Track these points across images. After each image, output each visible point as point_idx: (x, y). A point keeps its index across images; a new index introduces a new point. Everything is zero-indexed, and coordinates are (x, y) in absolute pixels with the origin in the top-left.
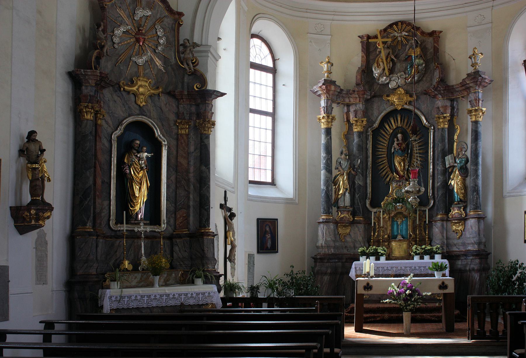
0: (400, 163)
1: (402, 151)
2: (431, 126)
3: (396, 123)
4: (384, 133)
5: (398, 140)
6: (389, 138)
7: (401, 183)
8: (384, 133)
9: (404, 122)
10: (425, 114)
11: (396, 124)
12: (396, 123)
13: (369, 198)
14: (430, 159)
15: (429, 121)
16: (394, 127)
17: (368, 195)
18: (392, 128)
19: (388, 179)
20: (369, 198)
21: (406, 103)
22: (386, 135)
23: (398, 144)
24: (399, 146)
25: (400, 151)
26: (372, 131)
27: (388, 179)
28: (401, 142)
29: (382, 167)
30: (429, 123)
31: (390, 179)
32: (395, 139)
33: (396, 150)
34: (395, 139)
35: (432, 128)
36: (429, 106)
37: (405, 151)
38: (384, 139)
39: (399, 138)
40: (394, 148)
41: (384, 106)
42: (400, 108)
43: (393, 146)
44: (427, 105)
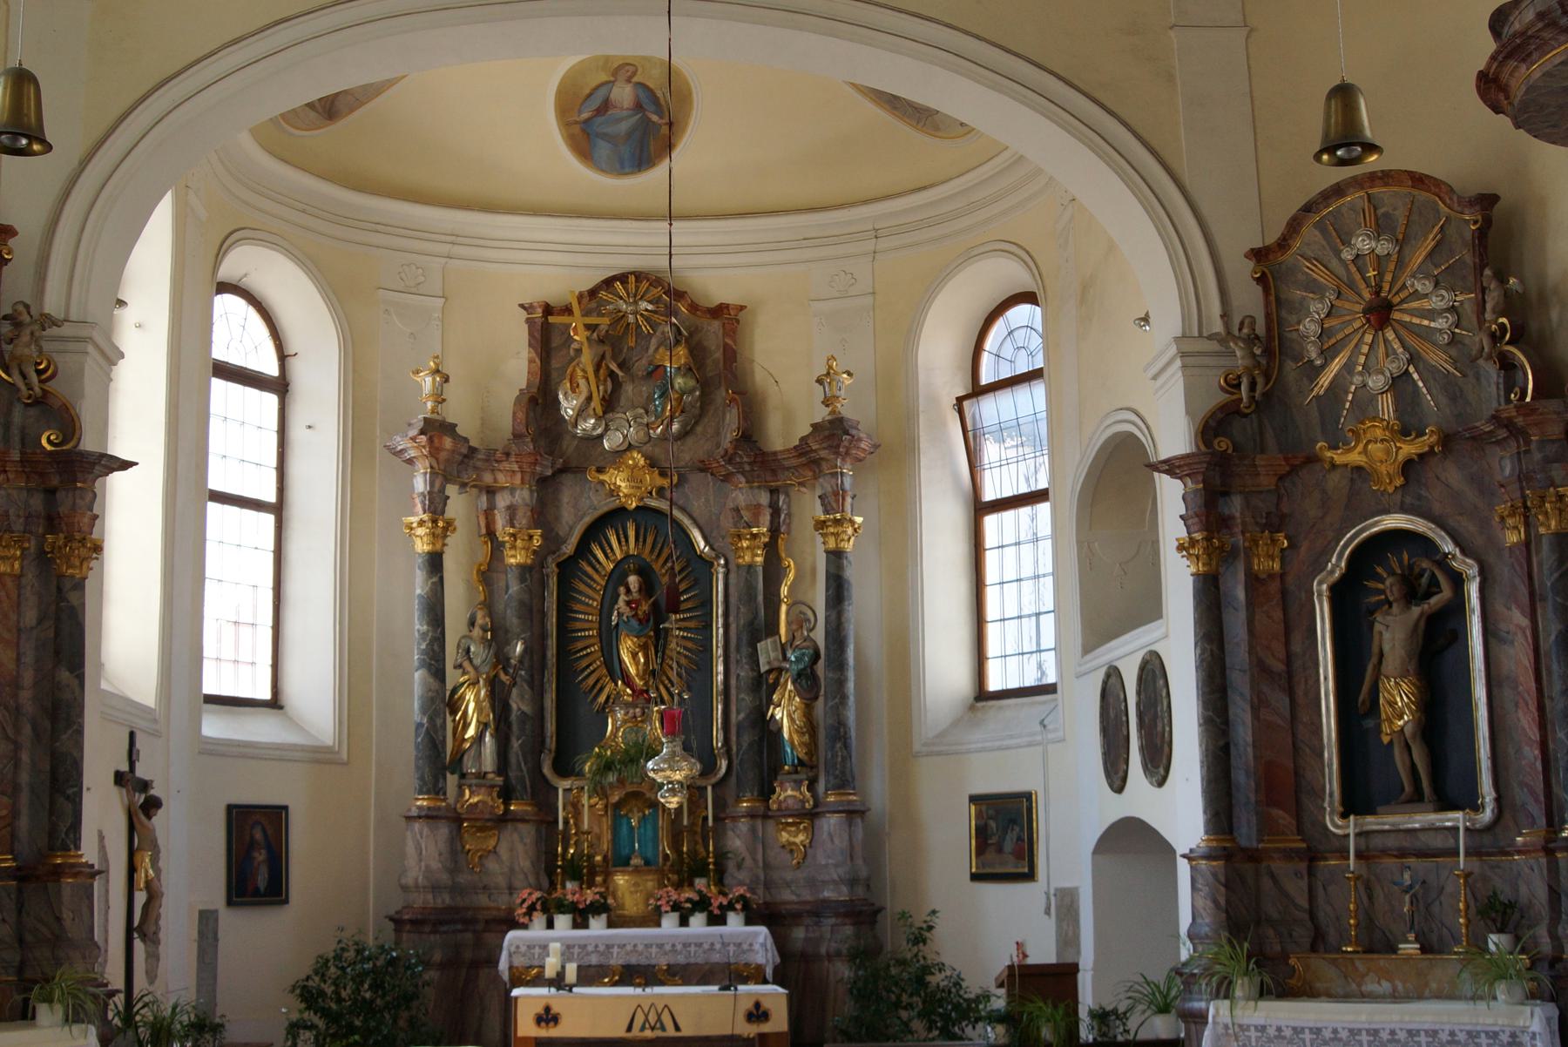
0: (634, 656)
1: (640, 621)
2: (718, 557)
3: (624, 543)
4: (589, 570)
5: (628, 591)
6: (603, 583)
7: (638, 710)
8: (589, 570)
9: (645, 541)
10: (702, 522)
11: (625, 548)
12: (624, 543)
13: (550, 751)
14: (717, 647)
15: (712, 541)
16: (619, 556)
17: (548, 740)
18: (612, 558)
19: (602, 699)
20: (550, 751)
21: (651, 493)
22: (596, 576)
23: (628, 603)
24: (631, 608)
25: (634, 623)
26: (559, 565)
27: (602, 699)
28: (636, 595)
29: (584, 663)
30: (712, 548)
31: (608, 697)
32: (622, 590)
33: (625, 618)
34: (622, 590)
35: (722, 562)
36: (712, 502)
37: (648, 621)
38: (590, 587)
39: (632, 587)
40: (618, 613)
41: (589, 497)
42: (634, 505)
43: (616, 607)
44: (707, 501)
